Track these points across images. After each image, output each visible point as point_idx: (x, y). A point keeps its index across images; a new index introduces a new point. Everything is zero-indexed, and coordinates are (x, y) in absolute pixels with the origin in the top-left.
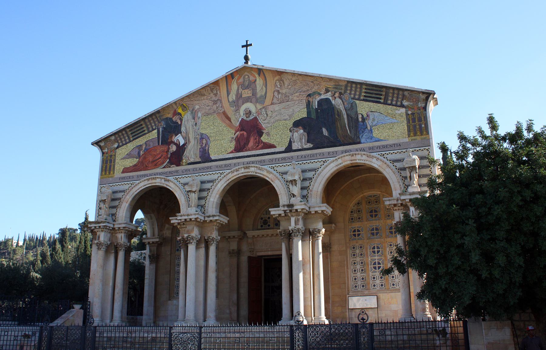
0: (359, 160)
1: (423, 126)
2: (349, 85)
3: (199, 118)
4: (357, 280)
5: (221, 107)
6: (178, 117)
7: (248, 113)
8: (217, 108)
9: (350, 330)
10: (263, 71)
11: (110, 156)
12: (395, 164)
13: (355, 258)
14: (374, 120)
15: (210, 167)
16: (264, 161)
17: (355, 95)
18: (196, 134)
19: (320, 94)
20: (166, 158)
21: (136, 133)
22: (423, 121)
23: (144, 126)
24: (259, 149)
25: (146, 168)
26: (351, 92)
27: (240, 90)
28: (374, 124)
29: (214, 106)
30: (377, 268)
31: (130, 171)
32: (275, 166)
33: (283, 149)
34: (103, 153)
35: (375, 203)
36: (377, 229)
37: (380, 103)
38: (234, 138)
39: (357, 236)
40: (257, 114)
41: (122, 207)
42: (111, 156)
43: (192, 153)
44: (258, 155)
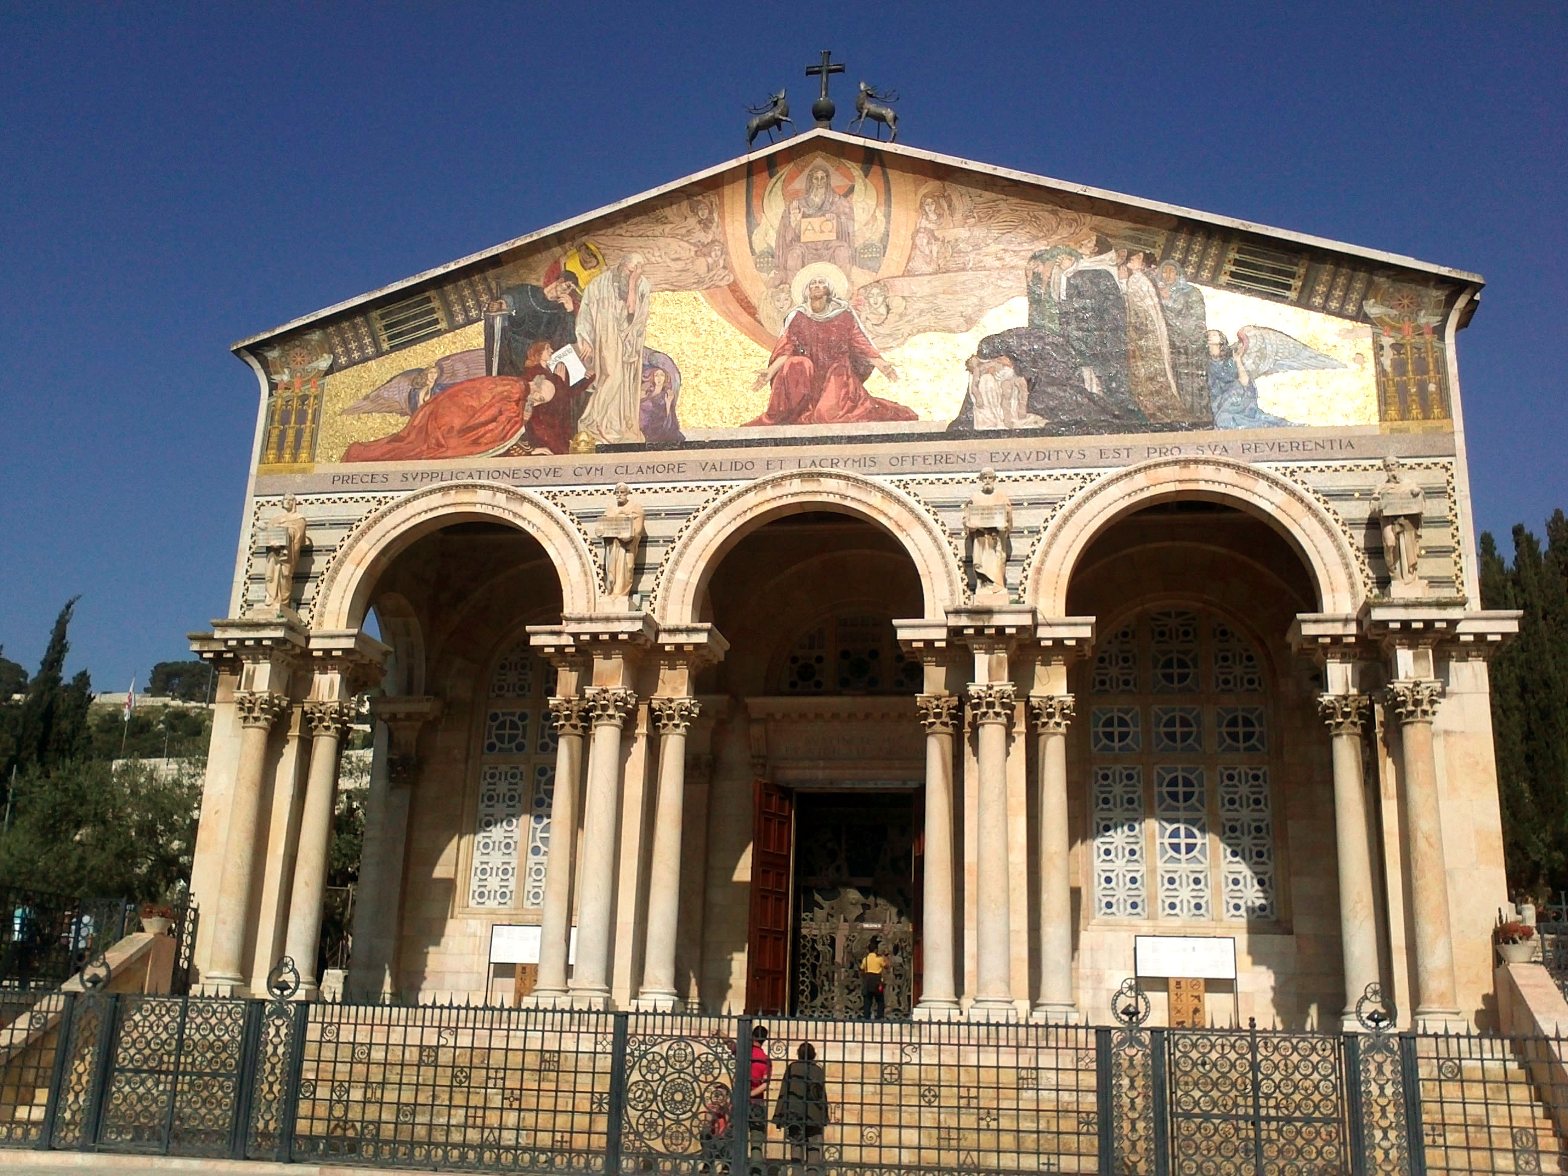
0: (1206, 481)
1: (1432, 387)
3: (642, 296)
4: (1113, 884)
5: (724, 267)
6: (564, 285)
7: (821, 298)
8: (709, 271)
9: (1327, 1053)
11: (299, 397)
12: (1332, 505)
13: (1110, 810)
14: (1262, 356)
15: (679, 467)
16: (873, 460)
17: (1199, 267)
18: (629, 349)
19: (1079, 257)
20: (516, 423)
21: (404, 327)
22: (1432, 374)
23: (435, 304)
24: (857, 421)
25: (437, 451)
26: (1186, 257)
27: (795, 217)
28: (1264, 367)
29: (697, 262)
30: (1183, 849)
31: (377, 453)
32: (912, 480)
34: (273, 387)
35: (1181, 638)
36: (1185, 723)
37: (1282, 299)
38: (770, 377)
39: (1116, 739)
40: (852, 303)
41: (339, 578)
42: (304, 398)
43: (613, 412)
44: (851, 440)
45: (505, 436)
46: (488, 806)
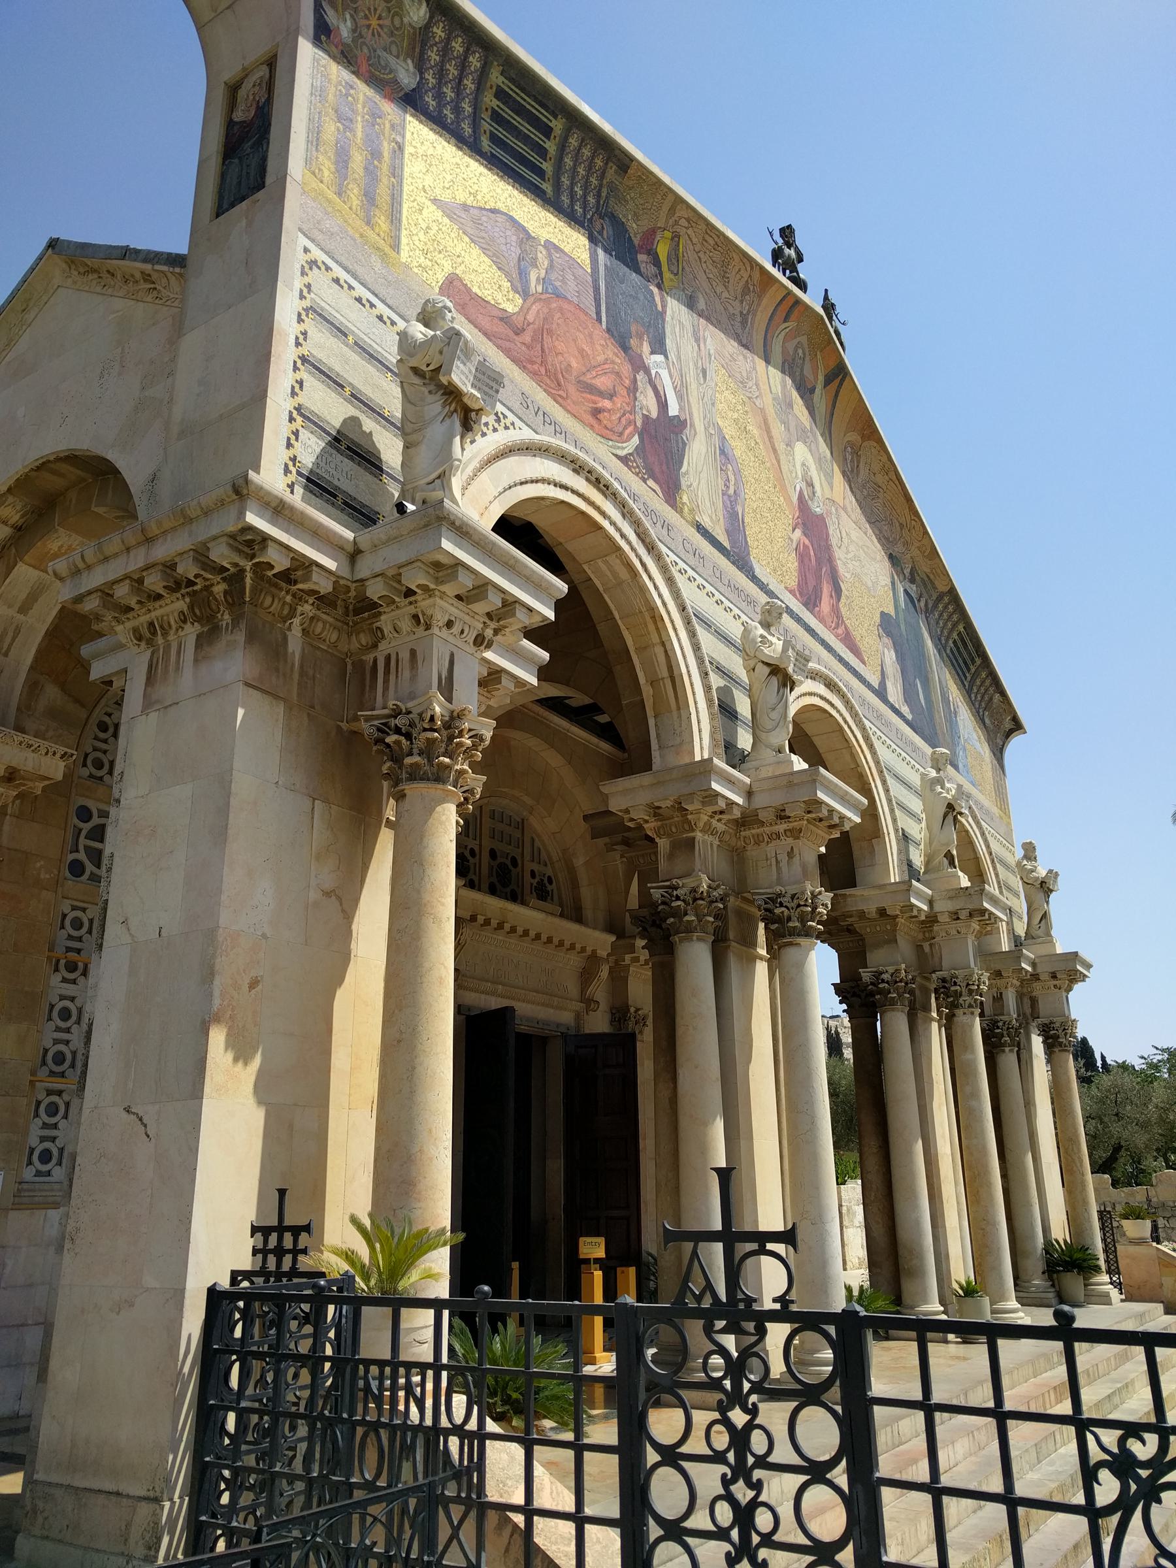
2: (946, 599)
10: (841, 384)
33: (875, 681)
44: (841, 660)
45: (621, 434)
46: (64, 980)
